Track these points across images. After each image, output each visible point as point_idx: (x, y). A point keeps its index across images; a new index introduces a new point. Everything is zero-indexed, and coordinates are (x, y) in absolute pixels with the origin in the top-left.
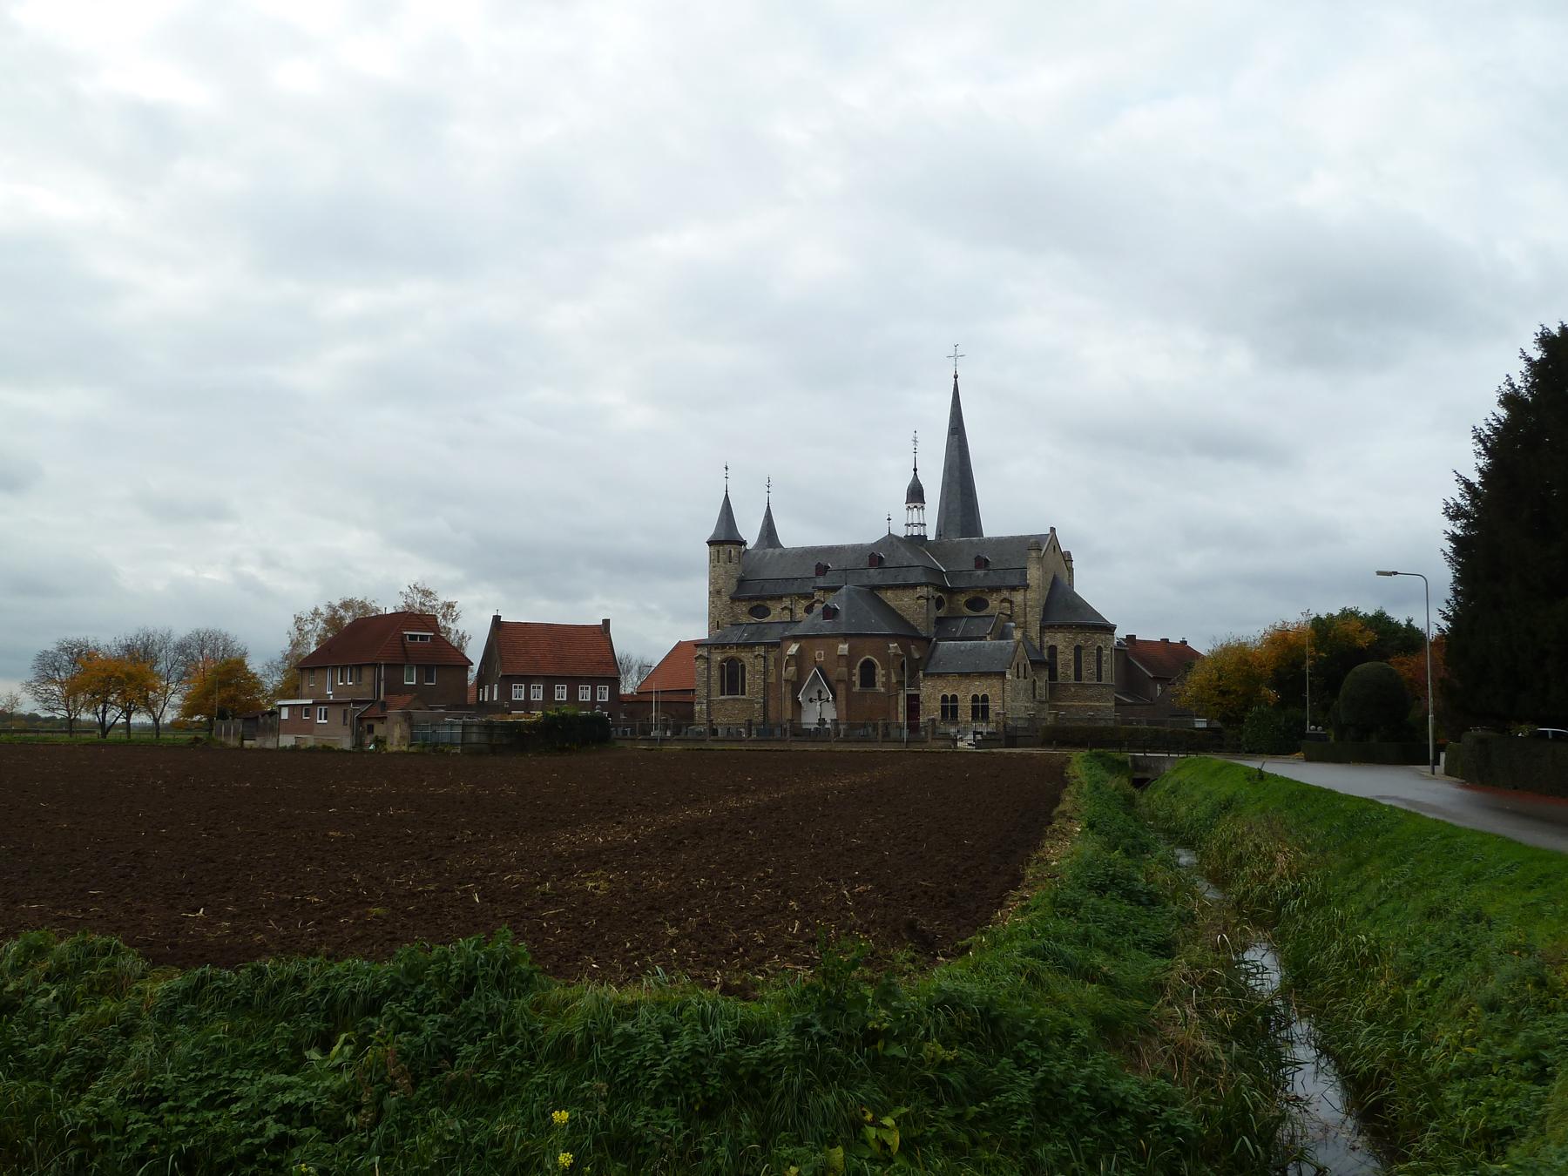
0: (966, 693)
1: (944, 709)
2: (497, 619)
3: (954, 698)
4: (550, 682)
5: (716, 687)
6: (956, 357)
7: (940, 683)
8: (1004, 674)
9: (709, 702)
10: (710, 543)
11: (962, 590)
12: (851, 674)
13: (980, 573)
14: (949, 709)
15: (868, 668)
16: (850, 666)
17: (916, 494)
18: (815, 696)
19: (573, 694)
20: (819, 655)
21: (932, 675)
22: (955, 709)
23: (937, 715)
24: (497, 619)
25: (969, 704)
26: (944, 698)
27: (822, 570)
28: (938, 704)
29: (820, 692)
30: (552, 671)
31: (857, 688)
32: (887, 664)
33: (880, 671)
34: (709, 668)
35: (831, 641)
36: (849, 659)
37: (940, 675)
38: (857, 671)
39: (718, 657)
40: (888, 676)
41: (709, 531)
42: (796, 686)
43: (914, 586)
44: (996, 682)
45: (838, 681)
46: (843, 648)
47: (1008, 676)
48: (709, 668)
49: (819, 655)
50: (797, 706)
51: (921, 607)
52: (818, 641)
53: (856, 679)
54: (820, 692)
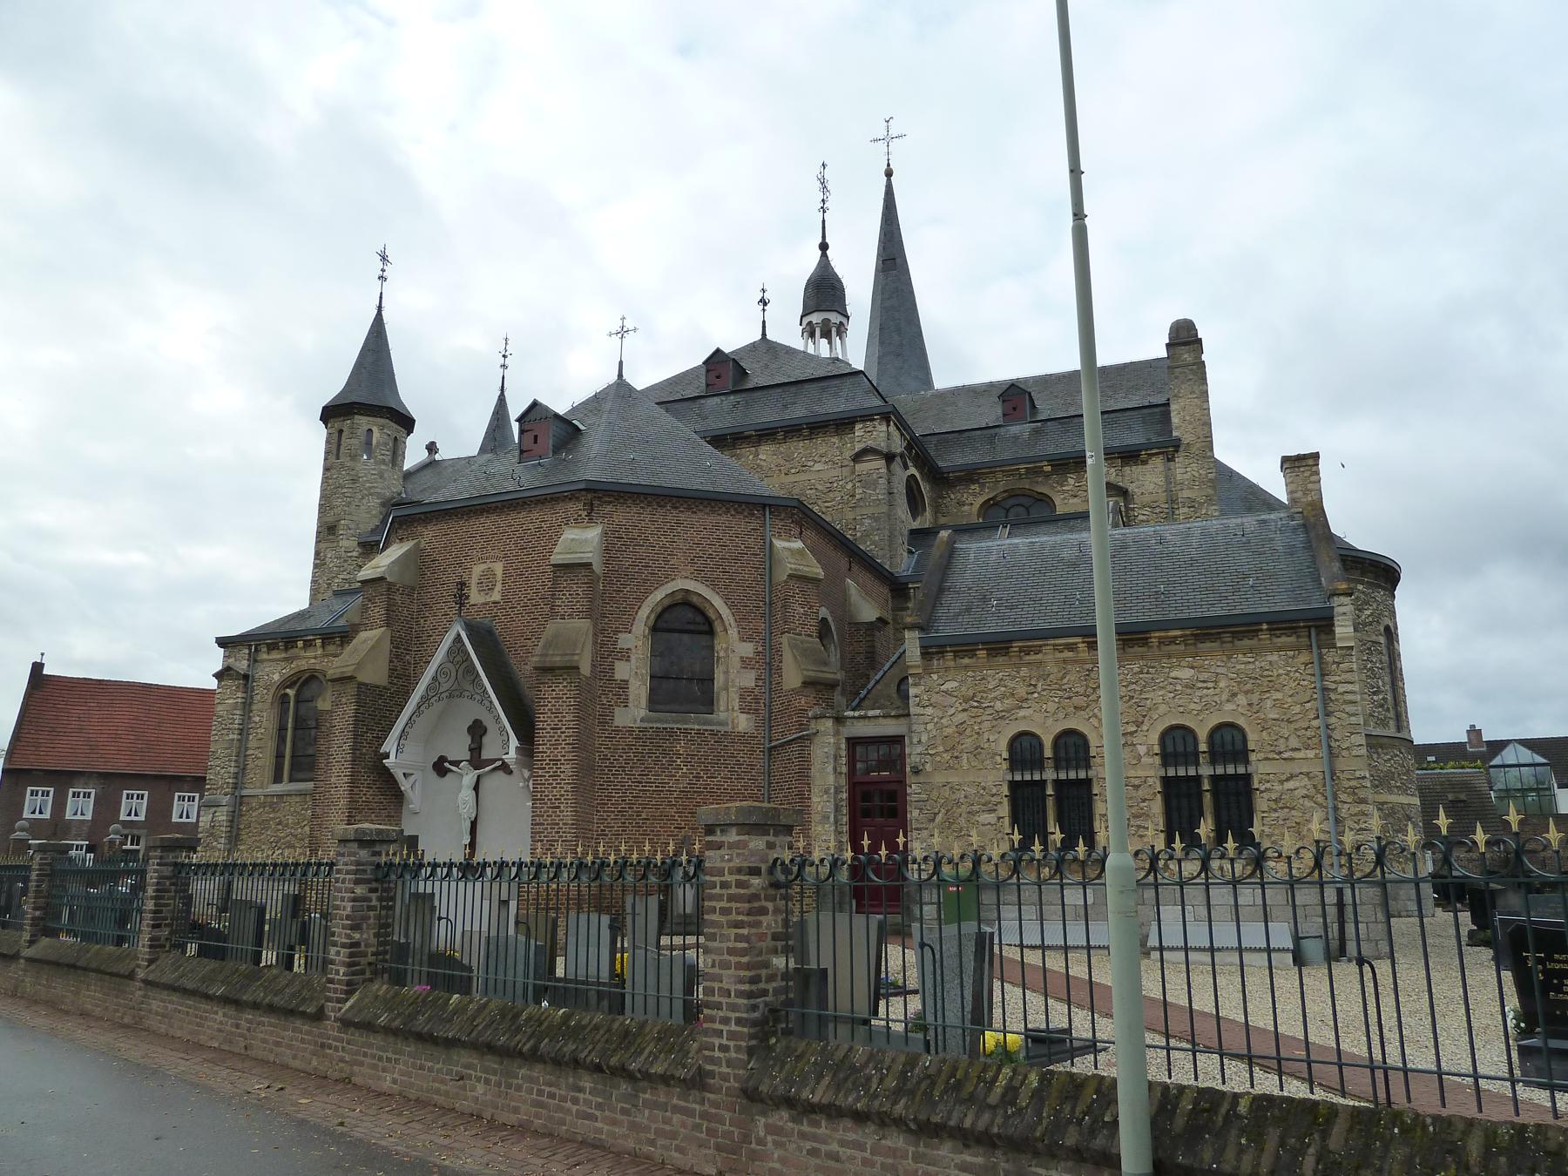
0: (1122, 728)
1: (1025, 804)
2: (37, 668)
3: (1073, 747)
4: (112, 782)
5: (262, 756)
6: (888, 139)
7: (998, 678)
8: (1323, 623)
9: (239, 801)
10: (329, 414)
11: (970, 476)
12: (607, 653)
13: (1021, 429)
14: (1051, 797)
15: (685, 623)
16: (605, 614)
17: (824, 292)
18: (459, 748)
19: (107, 807)
20: (488, 578)
21: (964, 647)
22: (1077, 806)
23: (993, 833)
24: (37, 668)
25: (1151, 771)
26: (1023, 751)
27: (662, 655)
28: (997, 777)
29: (477, 731)
30: (121, 765)
31: (634, 712)
32: (767, 609)
33: (734, 650)
34: (247, 706)
35: (531, 520)
36: (603, 589)
37: (998, 646)
38: (636, 639)
39: (273, 671)
40: (768, 663)
41: (333, 385)
42: (378, 708)
43: (843, 424)
44: (1283, 666)
45: (546, 670)
46: (581, 540)
47: (1343, 630)
48: (247, 706)
49: (488, 578)
50: (386, 788)
51: (868, 482)
52: (486, 524)
53: (634, 672)
54: (477, 731)
